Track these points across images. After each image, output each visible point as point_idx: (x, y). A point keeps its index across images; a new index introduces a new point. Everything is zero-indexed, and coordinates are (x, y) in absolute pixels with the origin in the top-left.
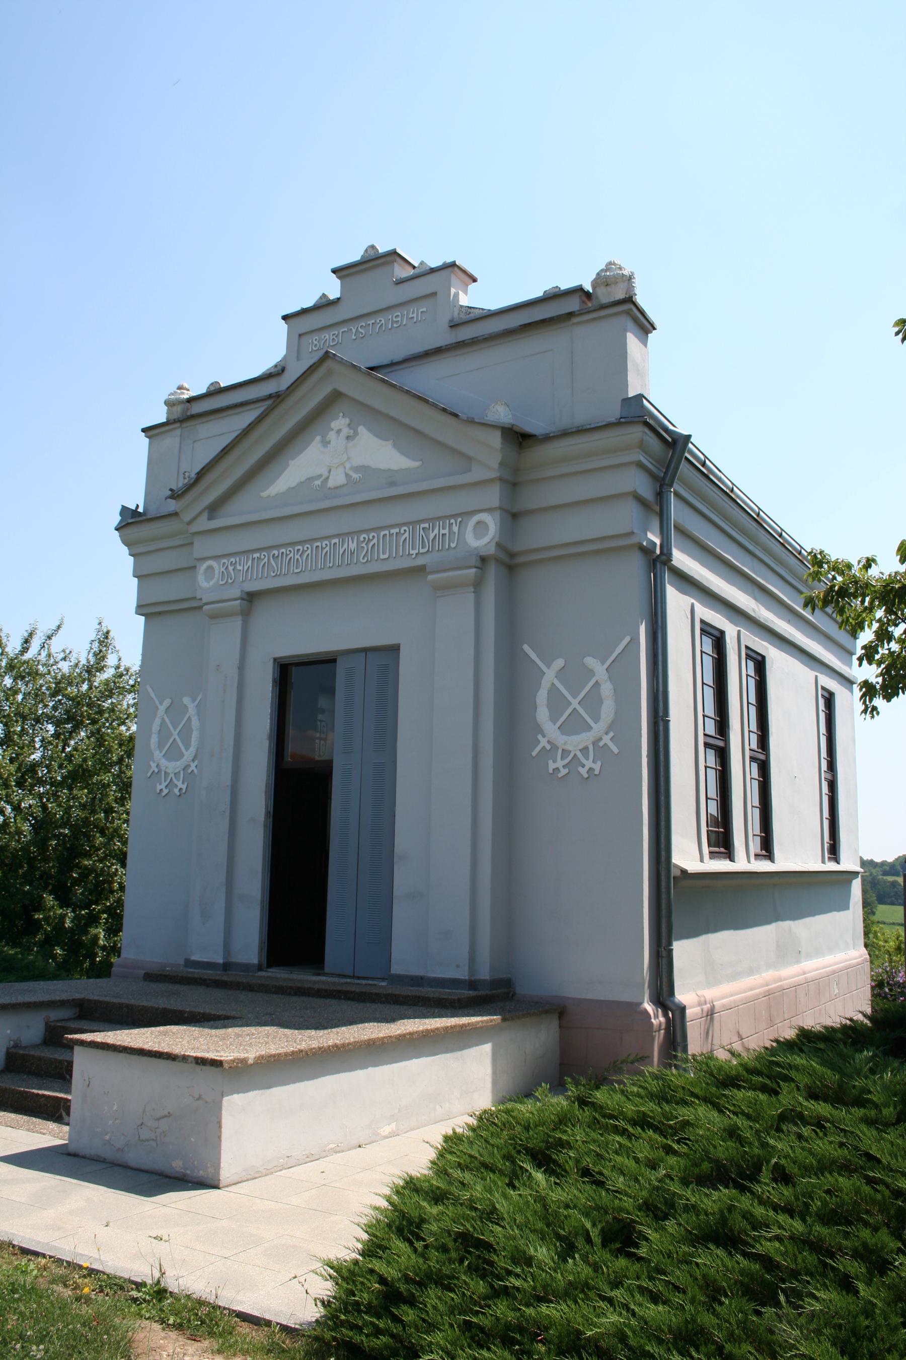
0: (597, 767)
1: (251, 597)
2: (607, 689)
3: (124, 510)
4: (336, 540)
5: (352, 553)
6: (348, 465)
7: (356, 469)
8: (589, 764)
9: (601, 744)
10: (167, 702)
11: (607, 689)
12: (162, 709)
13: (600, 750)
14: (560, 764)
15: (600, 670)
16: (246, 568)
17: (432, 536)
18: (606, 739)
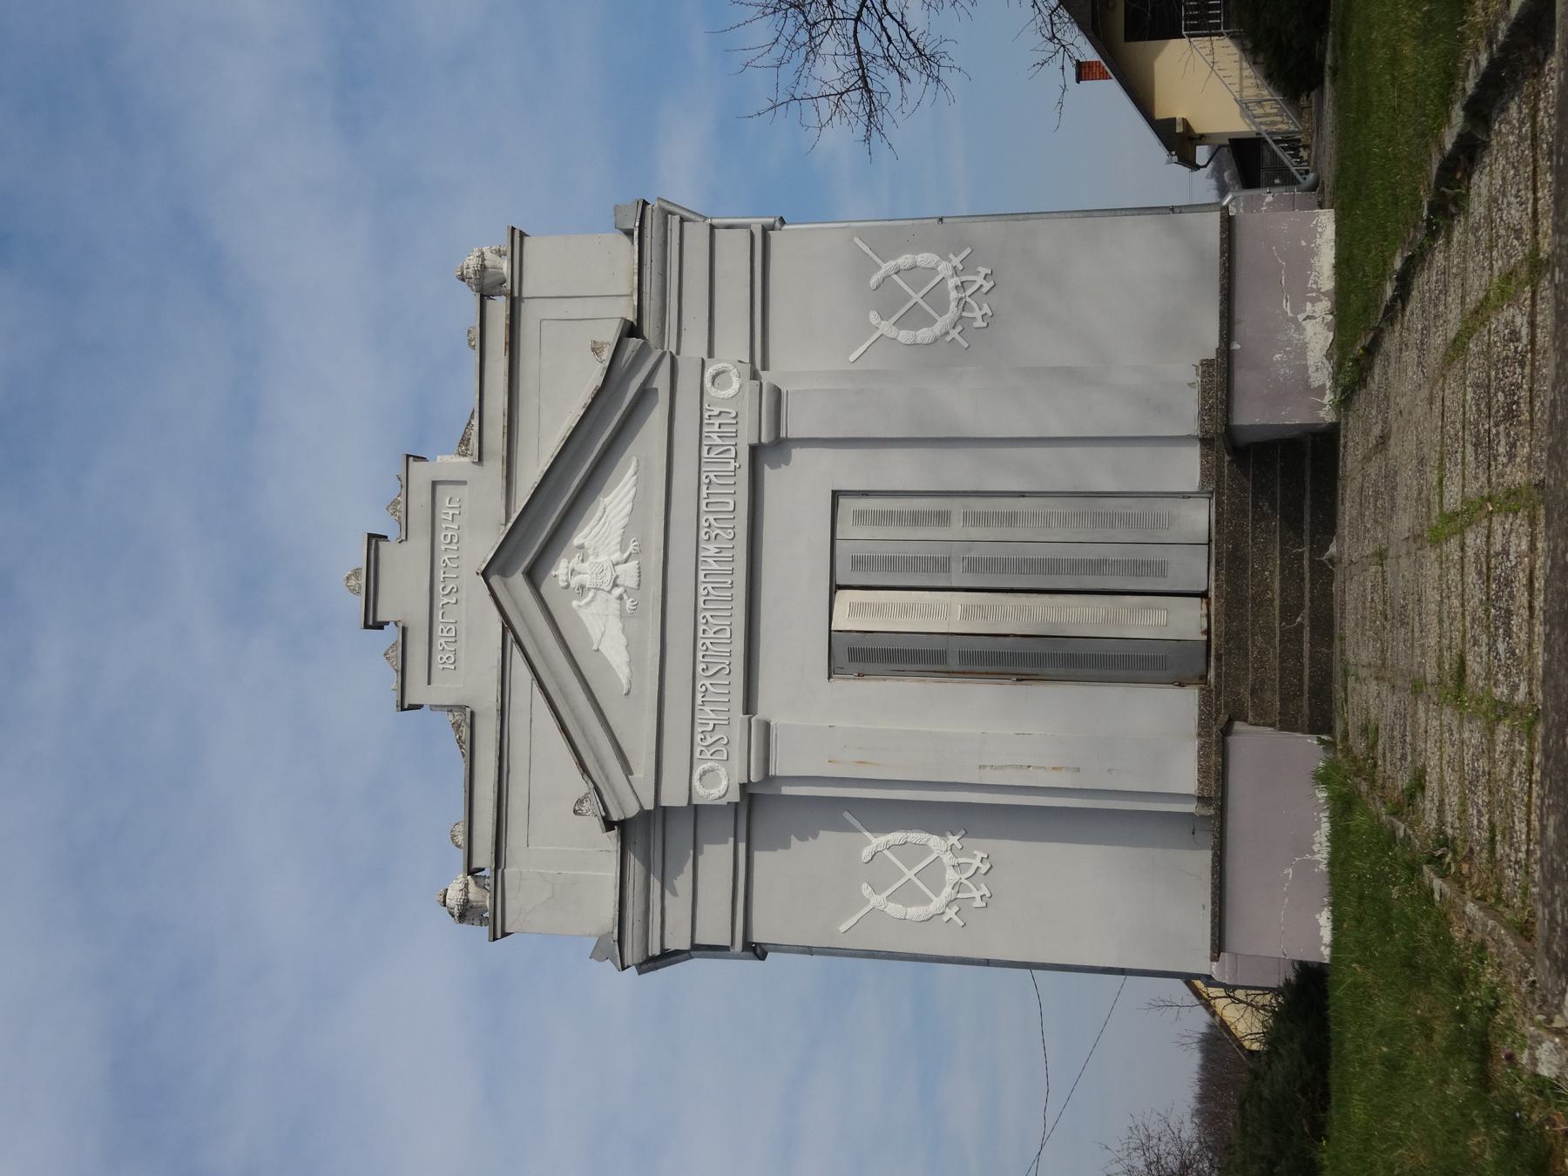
0: (984, 271)
1: (749, 707)
2: (904, 260)
3: (598, 954)
4: (701, 574)
5: (721, 550)
6: (617, 556)
7: (623, 546)
8: (980, 280)
9: (960, 267)
10: (866, 890)
11: (904, 260)
12: (876, 900)
13: (968, 266)
14: (978, 314)
15: (887, 267)
16: (712, 716)
17: (719, 441)
18: (956, 261)
